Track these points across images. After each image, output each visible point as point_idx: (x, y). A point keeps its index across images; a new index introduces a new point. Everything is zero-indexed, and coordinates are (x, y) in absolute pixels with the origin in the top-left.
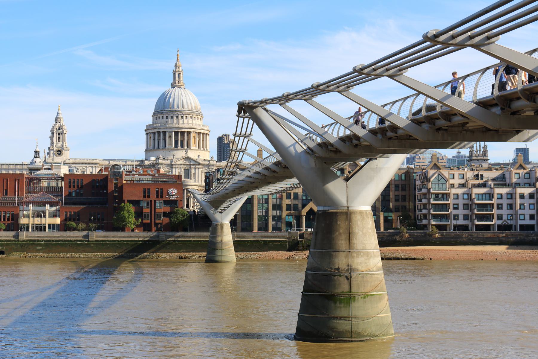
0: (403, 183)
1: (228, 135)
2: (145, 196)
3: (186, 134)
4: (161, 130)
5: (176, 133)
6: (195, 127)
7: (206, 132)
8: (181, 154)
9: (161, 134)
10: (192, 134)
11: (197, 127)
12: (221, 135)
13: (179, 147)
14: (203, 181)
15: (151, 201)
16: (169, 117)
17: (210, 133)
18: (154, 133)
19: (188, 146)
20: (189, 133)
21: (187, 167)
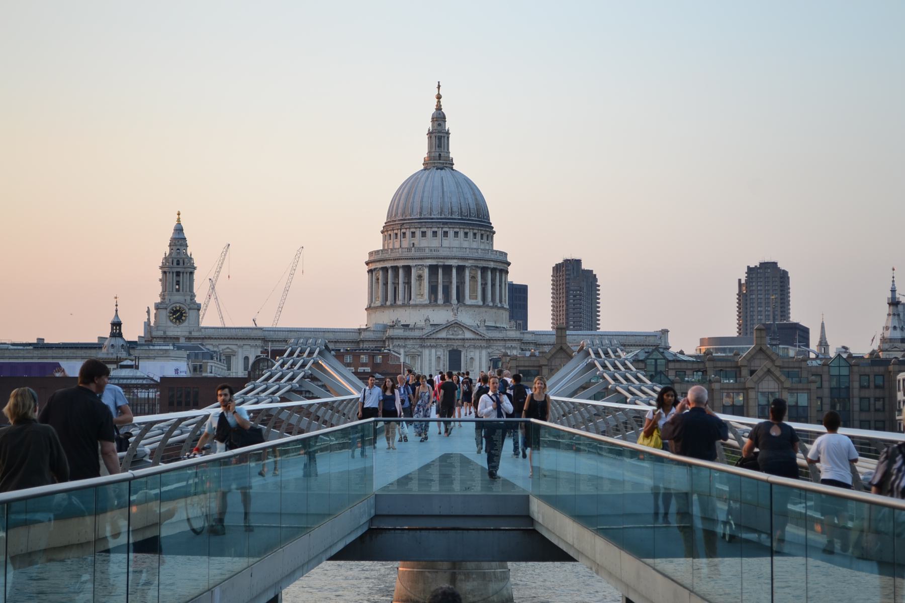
0: (878, 393)
1: (578, 262)
3: (454, 271)
4: (400, 263)
5: (433, 269)
6: (475, 255)
8: (441, 316)
9: (401, 272)
10: (467, 272)
11: (480, 254)
12: (561, 261)
13: (440, 300)
16: (418, 233)
18: (385, 270)
20: (461, 269)
21: (456, 345)
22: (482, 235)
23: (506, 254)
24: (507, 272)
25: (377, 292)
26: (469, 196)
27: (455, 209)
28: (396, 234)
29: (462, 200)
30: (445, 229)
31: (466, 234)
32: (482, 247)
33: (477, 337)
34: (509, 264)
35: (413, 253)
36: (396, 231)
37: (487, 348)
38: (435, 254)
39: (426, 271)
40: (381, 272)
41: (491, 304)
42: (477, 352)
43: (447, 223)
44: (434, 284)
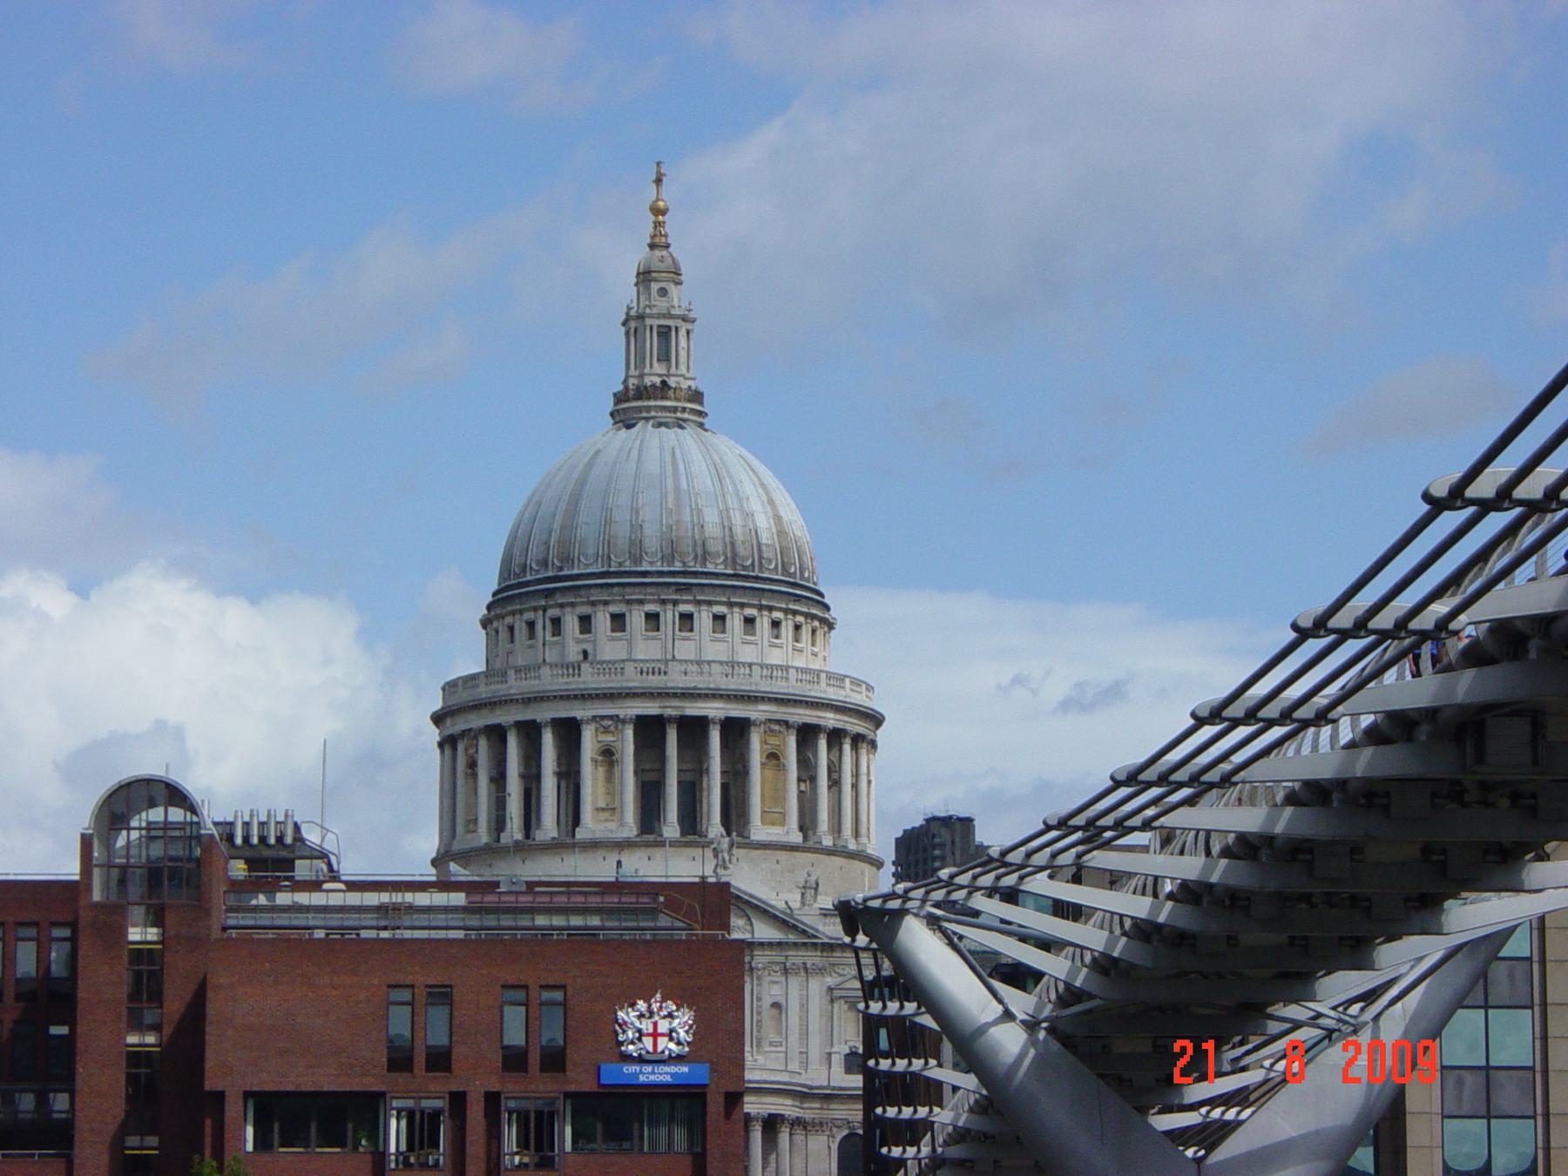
1: (967, 823)
2: (400, 1060)
3: (715, 737)
4: (543, 714)
5: (649, 731)
7: (855, 726)
9: (548, 738)
11: (791, 687)
12: (918, 822)
13: (671, 828)
14: (838, 1061)
15: (458, 1100)
16: (602, 620)
17: (881, 736)
18: (497, 734)
19: (735, 814)
20: (736, 730)
22: (797, 627)
23: (869, 688)
24: (873, 745)
25: (472, 806)
26: (757, 505)
27: (715, 547)
28: (531, 625)
29: (737, 521)
30: (684, 608)
31: (749, 621)
32: (800, 662)
33: (792, 938)
34: (876, 720)
35: (589, 679)
36: (529, 616)
37: (821, 971)
38: (655, 681)
39: (629, 732)
40: (483, 743)
41: (827, 841)
42: (795, 983)
43: (688, 588)
44: (651, 777)
